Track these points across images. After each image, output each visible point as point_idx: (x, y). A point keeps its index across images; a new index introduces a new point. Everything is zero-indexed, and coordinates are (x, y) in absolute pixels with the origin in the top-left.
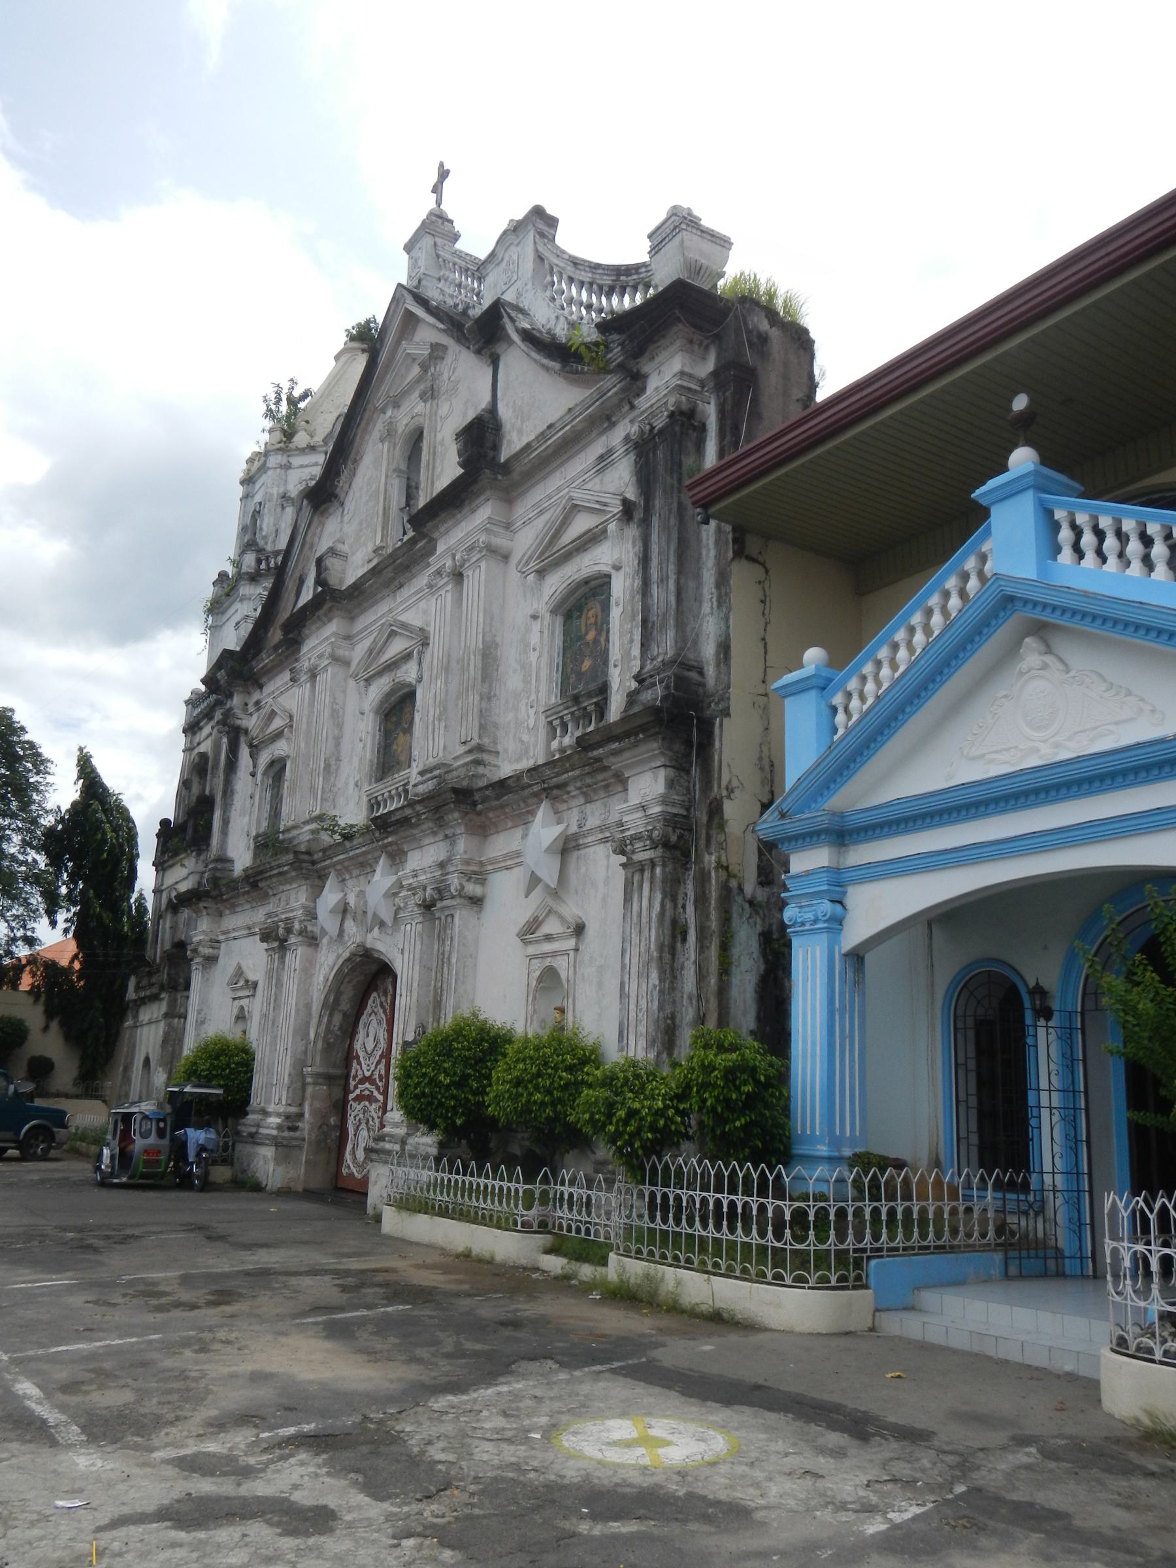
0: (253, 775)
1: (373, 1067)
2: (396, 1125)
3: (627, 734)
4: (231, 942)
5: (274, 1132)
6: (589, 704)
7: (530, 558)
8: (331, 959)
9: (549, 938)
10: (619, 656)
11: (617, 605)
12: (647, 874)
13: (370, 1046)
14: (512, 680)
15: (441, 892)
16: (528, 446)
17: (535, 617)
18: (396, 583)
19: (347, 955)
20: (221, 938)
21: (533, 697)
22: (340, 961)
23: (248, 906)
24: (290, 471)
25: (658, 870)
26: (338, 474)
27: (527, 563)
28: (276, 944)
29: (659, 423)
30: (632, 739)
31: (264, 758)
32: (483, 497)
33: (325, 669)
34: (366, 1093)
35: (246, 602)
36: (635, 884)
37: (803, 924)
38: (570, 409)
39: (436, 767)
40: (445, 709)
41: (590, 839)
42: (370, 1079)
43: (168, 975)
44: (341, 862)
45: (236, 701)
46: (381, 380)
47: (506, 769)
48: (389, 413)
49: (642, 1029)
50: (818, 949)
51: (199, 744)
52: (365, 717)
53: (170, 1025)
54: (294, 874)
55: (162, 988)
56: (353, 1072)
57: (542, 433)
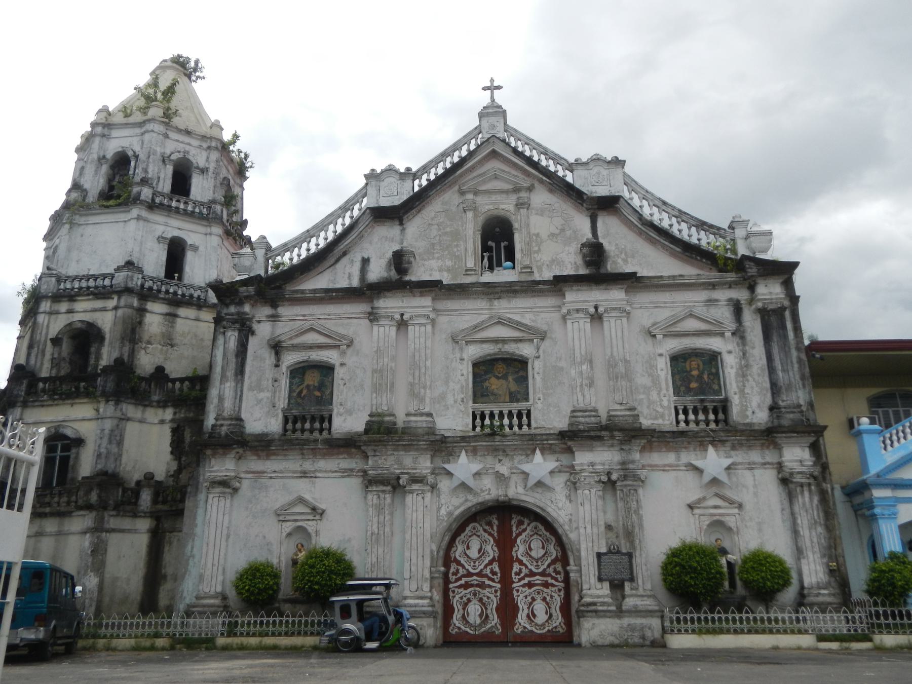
0: (277, 366)
1: (482, 567)
2: (599, 597)
3: (804, 432)
4: (263, 480)
5: (430, 609)
6: (710, 406)
7: (658, 327)
8: (456, 501)
9: (716, 507)
10: (737, 390)
11: (732, 368)
12: (805, 488)
13: (474, 553)
14: (642, 380)
15: (625, 477)
16: (661, 277)
17: (661, 355)
18: (497, 296)
19: (480, 500)
20: (243, 475)
21: (664, 392)
22: (469, 504)
23: (300, 457)
24: (167, 140)
25: (813, 488)
26: (412, 208)
27: (656, 329)
28: (389, 488)
29: (771, 307)
30: (806, 435)
31: (290, 359)
32: (619, 286)
33: (424, 325)
34: (476, 582)
35: (141, 223)
36: (798, 491)
37: (883, 515)
38: (698, 275)
39: (591, 411)
40: (593, 382)
41: (740, 467)
42: (480, 574)
43: (99, 496)
44: (473, 446)
45: (247, 308)
46: (461, 176)
47: (646, 422)
48: (470, 196)
49: (816, 549)
50: (893, 525)
51: (70, 311)
52: (465, 362)
53: (98, 537)
54: (425, 447)
55: (89, 507)
56: (452, 570)
57: (674, 277)
